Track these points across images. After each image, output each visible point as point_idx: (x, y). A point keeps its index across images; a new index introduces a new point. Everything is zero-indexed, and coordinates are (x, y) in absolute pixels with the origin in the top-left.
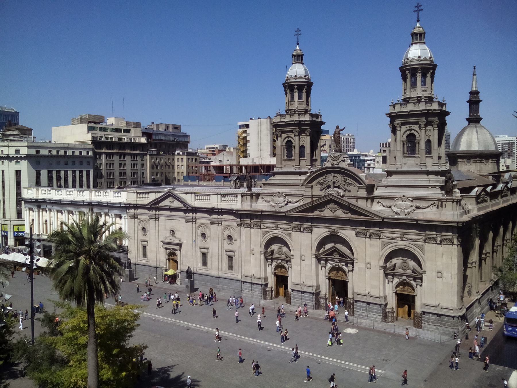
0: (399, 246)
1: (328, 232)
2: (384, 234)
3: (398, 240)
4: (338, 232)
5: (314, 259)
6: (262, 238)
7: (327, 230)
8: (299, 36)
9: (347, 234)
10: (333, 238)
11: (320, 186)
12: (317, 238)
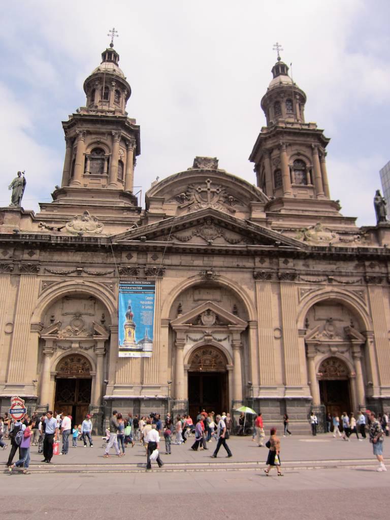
0: (328, 295)
1: (200, 275)
2: (301, 277)
3: (325, 285)
4: (220, 276)
5: (166, 331)
6: (39, 296)
7: (196, 273)
8: (115, 38)
9: (234, 280)
10: (208, 285)
11: (178, 203)
12: (173, 290)
